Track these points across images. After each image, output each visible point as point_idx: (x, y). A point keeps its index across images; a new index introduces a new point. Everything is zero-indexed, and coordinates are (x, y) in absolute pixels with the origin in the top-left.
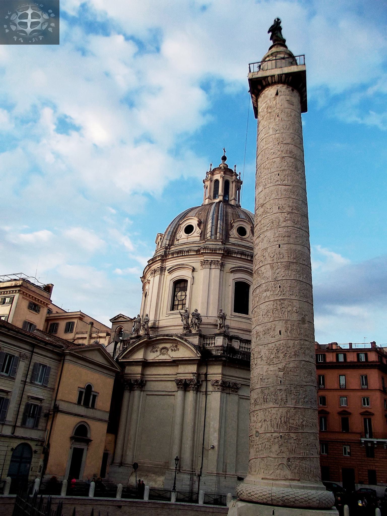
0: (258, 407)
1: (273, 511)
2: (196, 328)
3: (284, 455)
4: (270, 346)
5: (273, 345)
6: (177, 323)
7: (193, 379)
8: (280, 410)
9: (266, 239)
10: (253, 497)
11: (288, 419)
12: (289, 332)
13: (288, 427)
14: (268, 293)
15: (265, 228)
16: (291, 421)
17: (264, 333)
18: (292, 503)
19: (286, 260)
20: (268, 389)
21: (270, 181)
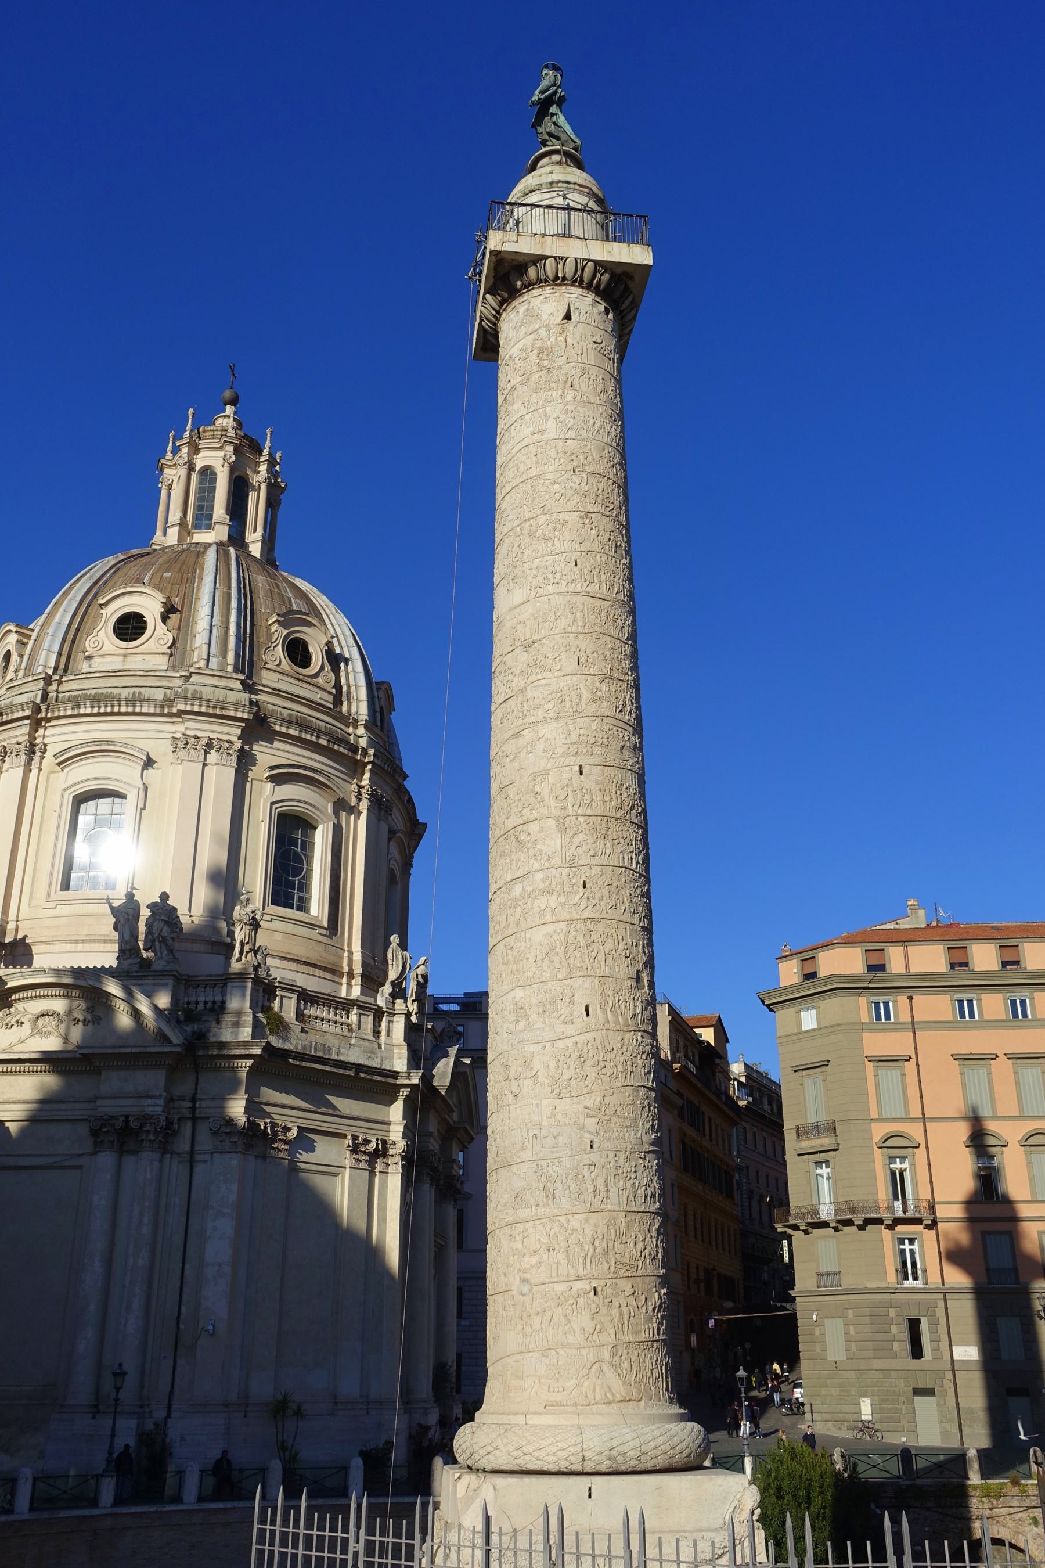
0: (524, 1213)
1: (590, 1489)
2: (161, 953)
3: (604, 1338)
4: (560, 1044)
5: (570, 1042)
6: (85, 932)
7: (152, 1116)
8: (592, 1221)
9: (542, 746)
10: (527, 1457)
11: (611, 1245)
12: (608, 1010)
13: (612, 1263)
14: (553, 900)
15: (540, 714)
16: (619, 1248)
17: (541, 1010)
18: (634, 1463)
19: (600, 811)
20: (557, 1164)
21: (551, 576)
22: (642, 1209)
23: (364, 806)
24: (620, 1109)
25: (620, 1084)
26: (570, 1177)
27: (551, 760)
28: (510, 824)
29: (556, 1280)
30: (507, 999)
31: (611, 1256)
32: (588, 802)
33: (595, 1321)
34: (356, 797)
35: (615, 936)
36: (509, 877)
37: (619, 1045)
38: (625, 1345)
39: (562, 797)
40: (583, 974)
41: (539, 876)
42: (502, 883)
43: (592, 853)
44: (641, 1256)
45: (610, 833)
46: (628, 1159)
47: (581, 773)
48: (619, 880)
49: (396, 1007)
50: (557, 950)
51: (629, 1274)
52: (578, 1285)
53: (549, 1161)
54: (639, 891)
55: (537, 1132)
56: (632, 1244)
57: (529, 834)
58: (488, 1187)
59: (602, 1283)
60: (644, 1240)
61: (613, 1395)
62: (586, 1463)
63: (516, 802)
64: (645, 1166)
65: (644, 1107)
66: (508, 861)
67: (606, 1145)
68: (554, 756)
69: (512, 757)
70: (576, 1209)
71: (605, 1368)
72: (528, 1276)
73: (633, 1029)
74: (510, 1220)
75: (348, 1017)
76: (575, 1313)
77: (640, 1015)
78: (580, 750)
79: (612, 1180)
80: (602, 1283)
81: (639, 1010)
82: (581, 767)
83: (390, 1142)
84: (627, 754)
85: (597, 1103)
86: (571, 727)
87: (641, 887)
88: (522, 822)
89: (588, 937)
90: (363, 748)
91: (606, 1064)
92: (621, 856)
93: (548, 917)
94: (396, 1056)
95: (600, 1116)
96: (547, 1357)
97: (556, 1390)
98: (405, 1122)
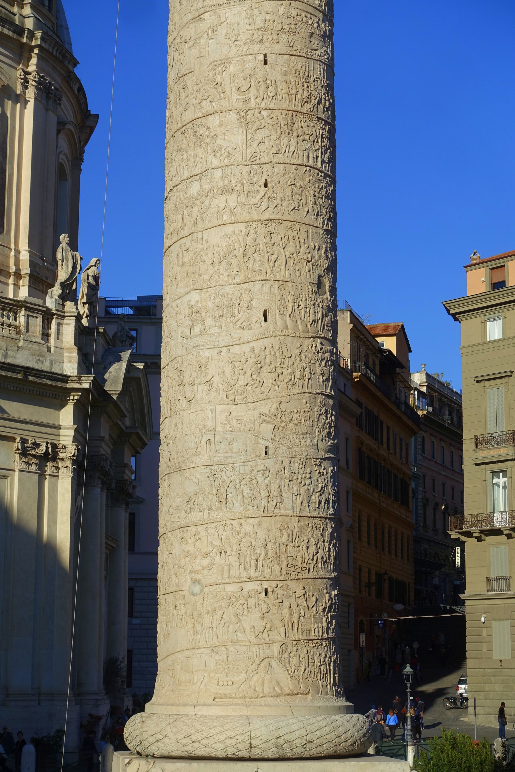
0: (196, 516)
3: (274, 636)
4: (236, 349)
5: (246, 348)
8: (265, 525)
9: (224, 32)
10: (196, 745)
11: (283, 548)
13: (284, 566)
14: (232, 200)
16: (291, 551)
17: (217, 314)
18: (299, 750)
19: (284, 105)
20: (231, 469)
22: (316, 514)
23: (31, 94)
24: (296, 416)
25: (297, 391)
26: (244, 482)
27: (234, 47)
28: (188, 116)
29: (227, 581)
30: (182, 302)
31: (283, 559)
32: (272, 94)
33: (265, 619)
34: (22, 84)
35: (296, 238)
36: (186, 174)
37: (298, 352)
38: (294, 643)
39: (244, 89)
40: (261, 278)
41: (218, 173)
42: (179, 180)
43: (274, 150)
44: (313, 559)
45: (294, 129)
46: (303, 465)
47: (266, 63)
48: (303, 180)
49: (66, 309)
50: (235, 252)
51: (300, 576)
52: (250, 586)
53: (222, 466)
54: (323, 191)
55: (211, 438)
56: (305, 548)
57: (208, 128)
58: (160, 490)
59: (274, 584)
60: (316, 544)
61: (281, 688)
62: (253, 750)
63: (195, 93)
64: (320, 473)
65: (321, 415)
66: (185, 157)
67: (281, 451)
68: (236, 43)
69: (191, 43)
70: (248, 514)
71: (274, 663)
72: (199, 577)
73: (312, 335)
74: (182, 523)
75: (15, 319)
76: (246, 613)
77: (320, 322)
78: (265, 37)
79: (286, 486)
80: (274, 584)
81: (319, 316)
82: (265, 55)
83: (61, 446)
84: (316, 42)
85: (273, 410)
86: (256, 11)
87: (326, 187)
88: (200, 115)
89: (268, 240)
90: (29, 30)
91: (284, 371)
92: (306, 154)
93: (226, 218)
94: (65, 360)
95: (276, 423)
96: (217, 653)
97: (225, 684)
98: (76, 426)
